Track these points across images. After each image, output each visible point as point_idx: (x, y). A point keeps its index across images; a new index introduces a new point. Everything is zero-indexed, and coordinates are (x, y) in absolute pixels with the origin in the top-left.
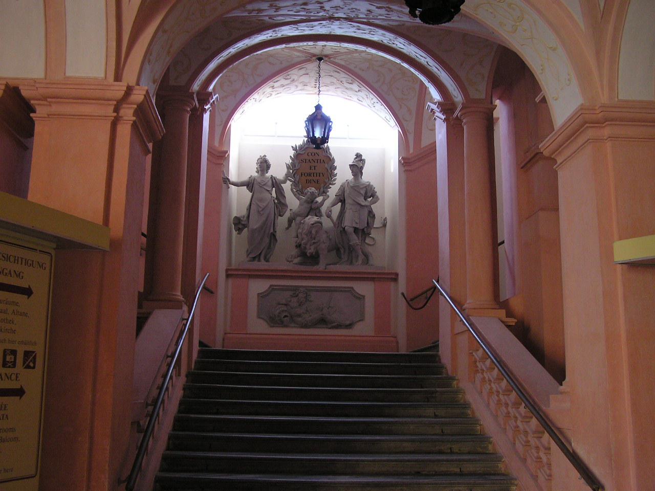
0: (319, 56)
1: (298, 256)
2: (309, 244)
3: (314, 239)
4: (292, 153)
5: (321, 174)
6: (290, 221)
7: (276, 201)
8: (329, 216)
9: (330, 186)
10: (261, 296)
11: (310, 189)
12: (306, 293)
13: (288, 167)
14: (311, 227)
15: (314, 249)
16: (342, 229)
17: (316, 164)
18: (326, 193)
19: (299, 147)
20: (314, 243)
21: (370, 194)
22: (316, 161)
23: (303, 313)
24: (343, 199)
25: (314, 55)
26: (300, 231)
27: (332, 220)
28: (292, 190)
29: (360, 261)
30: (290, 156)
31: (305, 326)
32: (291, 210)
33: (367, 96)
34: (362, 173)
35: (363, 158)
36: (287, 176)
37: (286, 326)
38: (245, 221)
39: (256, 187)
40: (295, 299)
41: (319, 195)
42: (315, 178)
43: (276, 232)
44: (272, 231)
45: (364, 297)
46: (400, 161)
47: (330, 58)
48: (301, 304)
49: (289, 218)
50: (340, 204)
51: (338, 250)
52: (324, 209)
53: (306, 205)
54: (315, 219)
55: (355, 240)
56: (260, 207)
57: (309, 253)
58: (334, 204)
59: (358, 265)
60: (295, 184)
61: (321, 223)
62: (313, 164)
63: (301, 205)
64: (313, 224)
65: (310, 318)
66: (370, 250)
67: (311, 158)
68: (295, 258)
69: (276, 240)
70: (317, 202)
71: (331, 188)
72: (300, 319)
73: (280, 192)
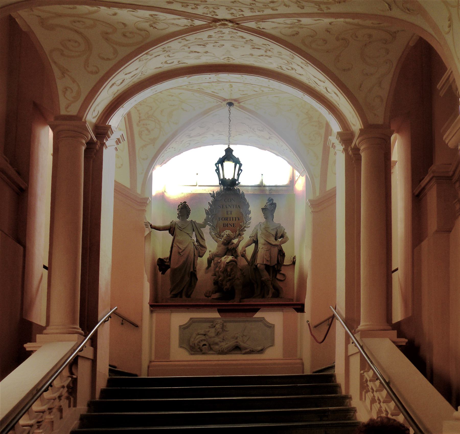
0: (229, 101)
1: (216, 292)
3: (230, 276)
6: (210, 261)
7: (196, 244)
8: (244, 256)
10: (183, 328)
12: (223, 324)
13: (207, 213)
14: (226, 265)
15: (230, 286)
16: (254, 267)
18: (241, 235)
20: (230, 280)
21: (280, 235)
23: (220, 342)
24: (256, 240)
25: (225, 100)
26: (217, 269)
27: (246, 259)
28: (210, 233)
31: (222, 352)
32: (210, 251)
33: (277, 143)
34: (273, 216)
35: (274, 202)
36: (206, 221)
37: (204, 354)
38: (168, 262)
39: (177, 231)
40: (213, 330)
41: (234, 238)
43: (196, 271)
44: (192, 270)
45: (274, 325)
47: (239, 103)
48: (218, 334)
49: (208, 259)
50: (254, 245)
52: (240, 248)
53: (223, 247)
54: (230, 258)
55: (266, 276)
56: (181, 249)
58: (248, 245)
59: (269, 298)
60: (214, 228)
61: (236, 262)
63: (218, 246)
64: (228, 263)
65: (226, 346)
66: (280, 284)
68: (213, 293)
69: (197, 279)
70: (233, 244)
71: (245, 230)
72: (217, 347)
73: (200, 236)
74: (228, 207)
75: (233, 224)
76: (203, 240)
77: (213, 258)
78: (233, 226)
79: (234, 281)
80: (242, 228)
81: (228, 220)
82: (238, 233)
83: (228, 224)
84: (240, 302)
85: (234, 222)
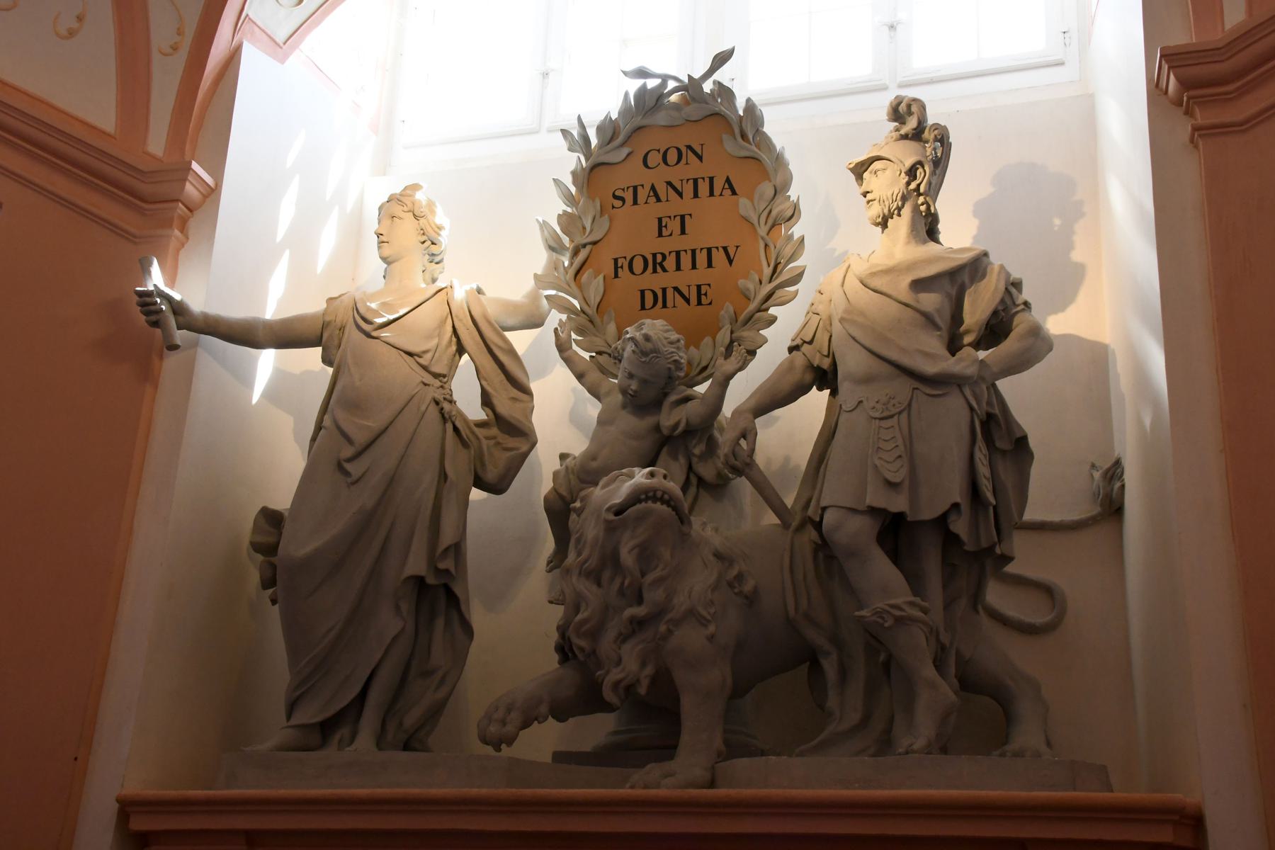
2: (610, 634)
4: (569, 162)
5: (719, 257)
9: (773, 311)
11: (640, 328)
14: (610, 528)
15: (643, 664)
17: (686, 205)
19: (600, 129)
20: (638, 624)
22: (688, 189)
29: (924, 728)
30: (557, 182)
42: (687, 279)
46: (1156, 90)
51: (812, 659)
53: (629, 422)
57: (616, 685)
62: (674, 206)
64: (619, 511)
67: (658, 177)
71: (773, 320)
74: (663, 198)
75: (699, 287)
76: (515, 393)
77: (571, 492)
78: (694, 300)
79: (670, 632)
80: (752, 306)
81: (664, 270)
82: (724, 336)
83: (664, 290)
84: (712, 784)
85: (702, 275)
